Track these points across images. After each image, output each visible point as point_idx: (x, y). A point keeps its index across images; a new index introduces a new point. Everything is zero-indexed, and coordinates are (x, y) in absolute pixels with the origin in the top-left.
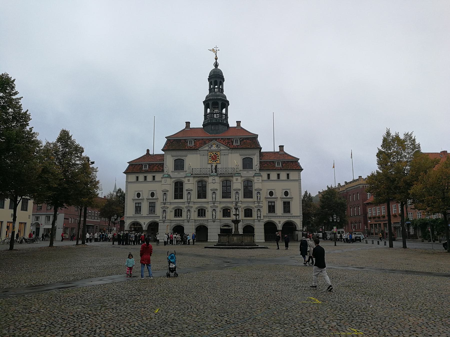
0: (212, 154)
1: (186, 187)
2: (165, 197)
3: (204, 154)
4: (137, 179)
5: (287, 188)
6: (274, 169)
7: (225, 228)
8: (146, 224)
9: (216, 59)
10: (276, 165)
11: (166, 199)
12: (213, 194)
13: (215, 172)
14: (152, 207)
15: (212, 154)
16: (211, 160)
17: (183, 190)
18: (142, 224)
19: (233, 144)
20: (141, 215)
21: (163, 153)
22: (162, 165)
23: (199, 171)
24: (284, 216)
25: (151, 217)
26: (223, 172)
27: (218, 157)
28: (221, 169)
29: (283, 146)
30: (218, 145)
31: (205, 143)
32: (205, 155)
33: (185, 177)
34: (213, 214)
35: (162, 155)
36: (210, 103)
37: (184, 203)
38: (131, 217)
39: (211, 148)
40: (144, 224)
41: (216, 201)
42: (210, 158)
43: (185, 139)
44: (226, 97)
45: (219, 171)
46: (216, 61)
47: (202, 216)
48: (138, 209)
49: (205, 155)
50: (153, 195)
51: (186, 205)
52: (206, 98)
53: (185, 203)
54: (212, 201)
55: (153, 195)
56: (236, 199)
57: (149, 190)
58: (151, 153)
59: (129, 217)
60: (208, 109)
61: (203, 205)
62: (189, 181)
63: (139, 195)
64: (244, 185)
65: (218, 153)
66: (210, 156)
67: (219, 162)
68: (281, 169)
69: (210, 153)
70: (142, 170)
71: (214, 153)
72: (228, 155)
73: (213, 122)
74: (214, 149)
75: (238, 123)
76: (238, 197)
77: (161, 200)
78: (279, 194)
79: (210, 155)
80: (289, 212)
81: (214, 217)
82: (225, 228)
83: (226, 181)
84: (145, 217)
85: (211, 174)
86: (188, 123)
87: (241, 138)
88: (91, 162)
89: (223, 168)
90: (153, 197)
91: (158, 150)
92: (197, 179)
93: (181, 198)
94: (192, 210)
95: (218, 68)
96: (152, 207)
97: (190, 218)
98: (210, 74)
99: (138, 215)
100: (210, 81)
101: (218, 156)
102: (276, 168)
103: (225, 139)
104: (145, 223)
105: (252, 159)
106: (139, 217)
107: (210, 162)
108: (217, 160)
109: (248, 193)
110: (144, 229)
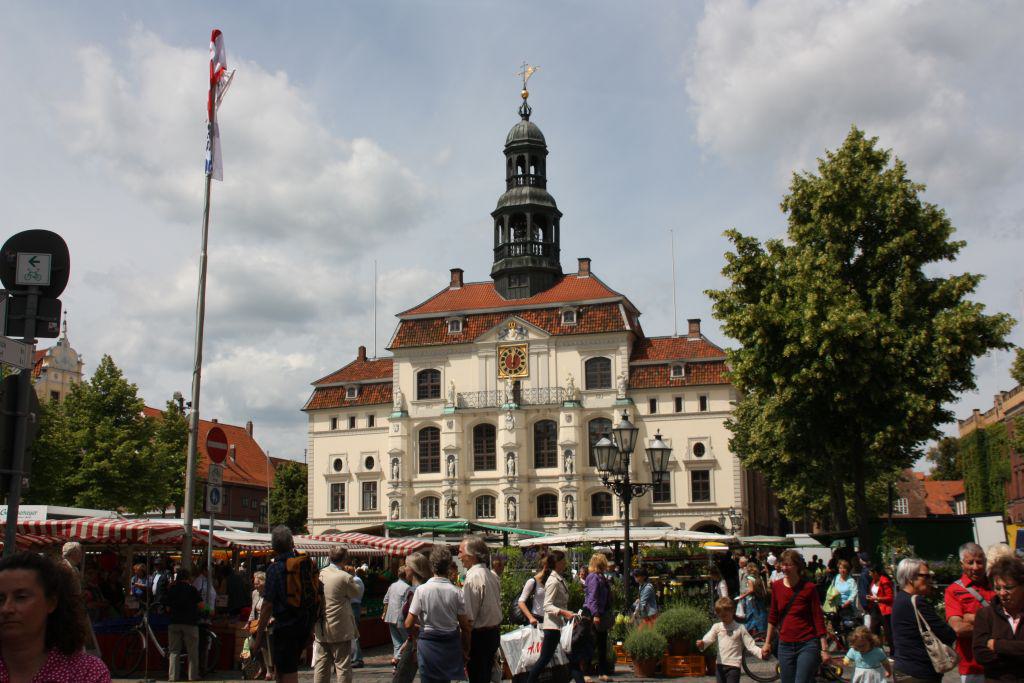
1: (447, 440)
4: (334, 426)
5: (702, 436)
6: (669, 386)
9: (525, 97)
10: (672, 375)
14: (370, 489)
17: (438, 449)
19: (559, 323)
21: (390, 354)
22: (388, 387)
24: (693, 511)
25: (368, 518)
26: (535, 400)
30: (521, 330)
31: (490, 325)
32: (491, 356)
33: (442, 417)
35: (389, 362)
36: (507, 218)
37: (440, 482)
38: (323, 520)
39: (506, 338)
41: (516, 474)
43: (442, 318)
44: (553, 202)
45: (528, 396)
46: (525, 104)
47: (487, 514)
48: (338, 498)
49: (491, 356)
50: (370, 462)
51: (444, 489)
52: (500, 202)
55: (370, 462)
57: (363, 451)
58: (370, 355)
59: (318, 520)
62: (450, 425)
63: (338, 464)
64: (593, 431)
67: (525, 372)
68: (683, 385)
70: (344, 402)
72: (548, 353)
73: (513, 266)
74: (513, 339)
75: (585, 262)
77: (388, 476)
78: (681, 453)
80: (707, 496)
81: (511, 517)
86: (457, 273)
87: (581, 306)
88: (187, 404)
89: (534, 389)
90: (371, 468)
91: (377, 351)
92: (472, 421)
93: (436, 468)
95: (531, 119)
96: (370, 489)
98: (508, 140)
99: (338, 514)
101: (523, 358)
102: (672, 382)
103: (542, 310)
105: (609, 361)
106: (340, 519)
108: (520, 369)
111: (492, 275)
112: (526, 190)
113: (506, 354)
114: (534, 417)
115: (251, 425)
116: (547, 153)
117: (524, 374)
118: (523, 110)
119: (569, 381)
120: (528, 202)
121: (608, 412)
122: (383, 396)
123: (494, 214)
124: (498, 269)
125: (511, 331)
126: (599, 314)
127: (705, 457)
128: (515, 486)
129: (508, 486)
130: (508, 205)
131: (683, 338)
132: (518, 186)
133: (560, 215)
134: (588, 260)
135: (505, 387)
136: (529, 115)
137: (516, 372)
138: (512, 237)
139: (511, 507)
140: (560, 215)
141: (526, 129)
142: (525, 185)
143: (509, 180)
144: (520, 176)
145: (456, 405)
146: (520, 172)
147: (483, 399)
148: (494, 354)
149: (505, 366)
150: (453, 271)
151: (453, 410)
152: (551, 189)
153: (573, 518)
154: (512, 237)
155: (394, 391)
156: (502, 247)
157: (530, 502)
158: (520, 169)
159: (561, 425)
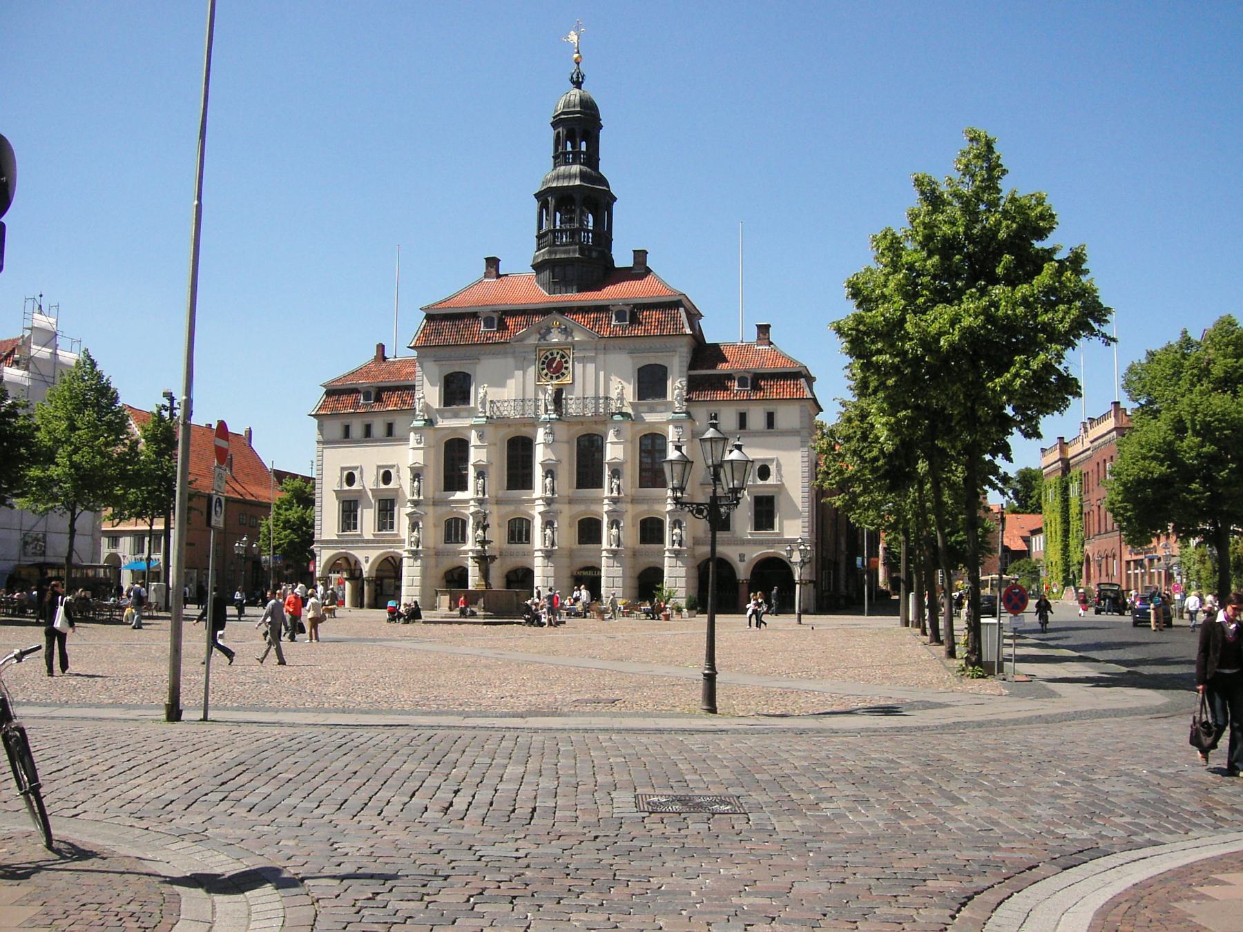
0: (548, 354)
1: (476, 455)
2: (416, 483)
7: (585, 573)
8: (370, 561)
11: (419, 491)
13: (555, 411)
18: (362, 560)
20: (359, 535)
26: (579, 410)
27: (565, 365)
29: (768, 327)
36: (552, 202)
40: (367, 561)
42: (543, 369)
50: (387, 478)
60: (557, 213)
63: (350, 479)
64: (643, 448)
65: (567, 351)
73: (558, 257)
75: (640, 256)
76: (619, 486)
79: (543, 359)
82: (585, 573)
84: (368, 541)
85: (543, 416)
93: (464, 487)
94: (492, 521)
100: (556, 131)
104: (367, 560)
105: (666, 368)
108: (563, 374)
109: (651, 474)
110: (365, 575)
111: (533, 266)
112: (576, 169)
113: (547, 357)
114: (580, 430)
115: (250, 432)
116: (601, 127)
117: (567, 380)
118: (575, 76)
119: (618, 391)
120: (578, 182)
121: (662, 426)
122: (404, 402)
123: (537, 196)
124: (540, 260)
125: (555, 332)
126: (656, 315)
127: (772, 480)
130: (554, 185)
131: (749, 345)
132: (567, 163)
133: (615, 199)
134: (645, 252)
135: (546, 397)
136: (582, 82)
137: (558, 378)
138: (558, 223)
139: (548, 531)
140: (615, 199)
141: (578, 98)
142: (574, 163)
143: (555, 158)
144: (569, 153)
145: (488, 414)
146: (569, 149)
147: (519, 408)
149: (545, 371)
150: (487, 259)
151: (485, 419)
152: (603, 169)
154: (558, 223)
155: (417, 396)
156: (545, 234)
157: (570, 526)
158: (569, 144)
159: (609, 440)
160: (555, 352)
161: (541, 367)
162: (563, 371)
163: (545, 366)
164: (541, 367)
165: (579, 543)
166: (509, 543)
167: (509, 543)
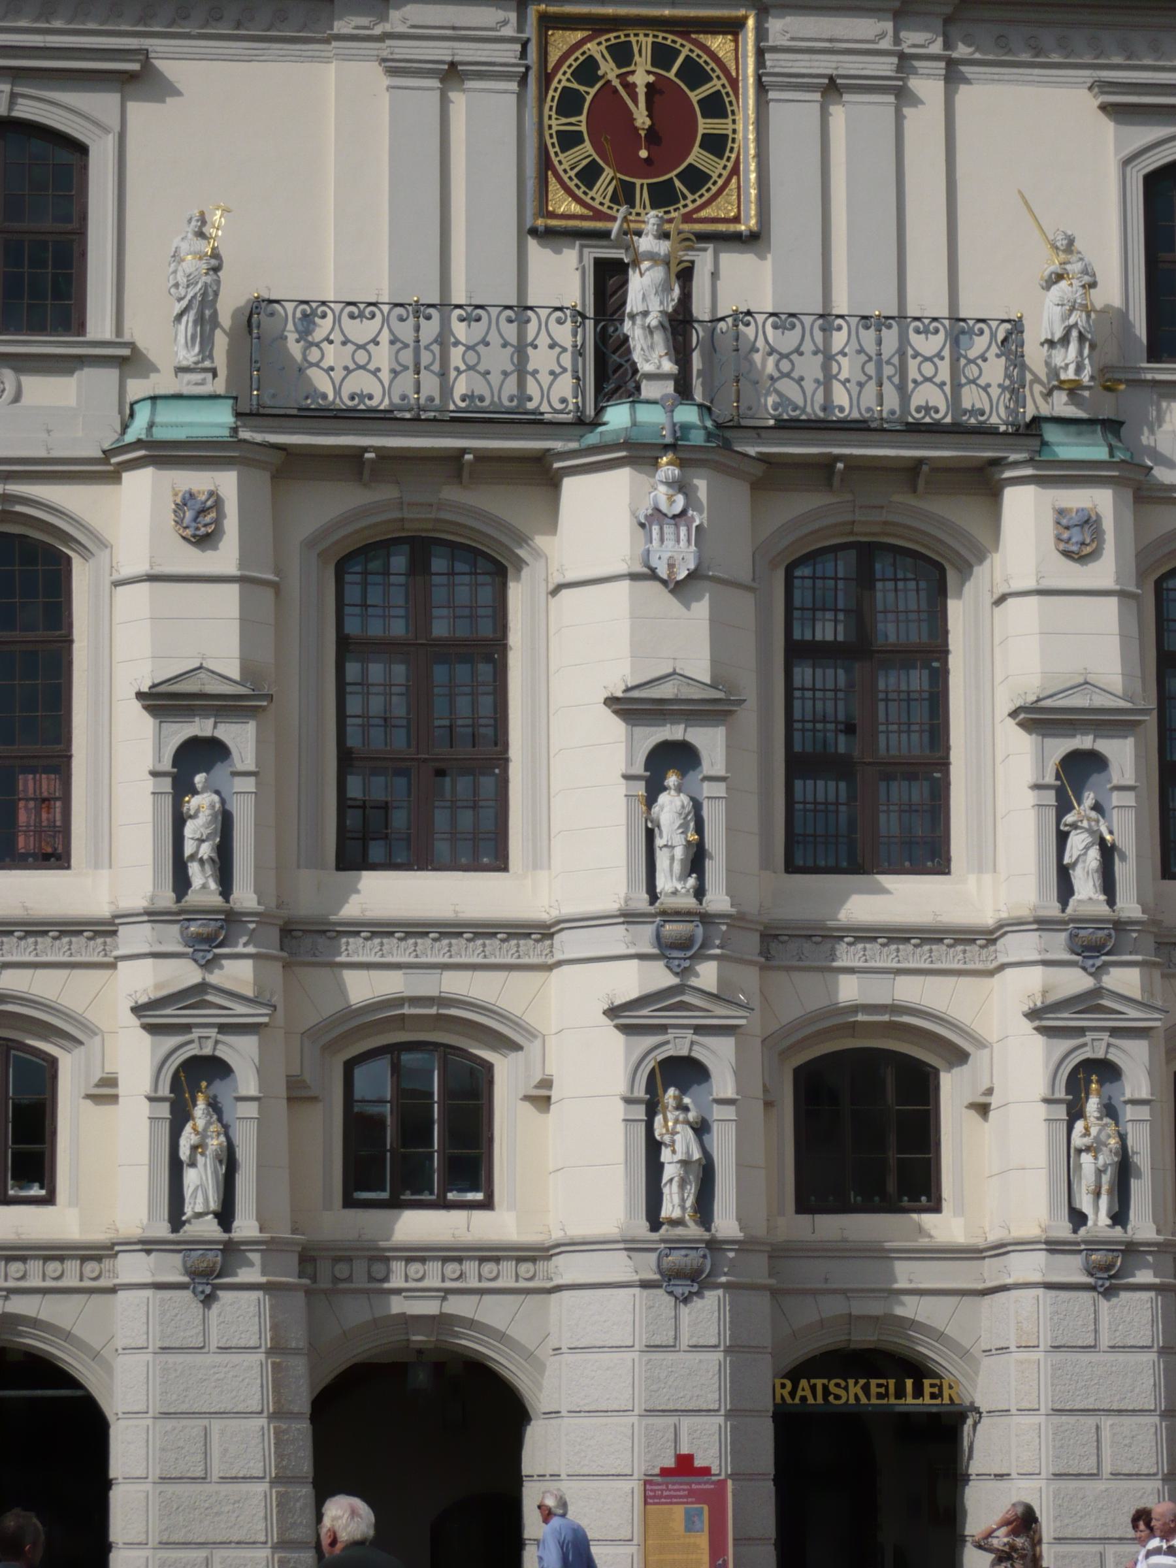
3: (467, 52)
12: (654, 789)
15: (609, 69)
16: (589, 175)
23: (382, 356)
27: (704, 126)
28: (787, 341)
34: (653, 1147)
42: (568, 140)
53: (134, 938)
54: (641, 901)
56: (1064, 875)
61: (454, 984)
66: (569, 103)
69: (561, 41)
71: (643, 43)
79: (562, 80)
83: (844, 566)
97: (225, 1216)
107: (562, 204)
108: (696, 179)
113: (587, 71)
128: (707, 975)
129: (661, 977)
137: (663, 197)
148: (508, 54)
153: (1119, 1217)
160: (643, 43)
161: (557, 124)
162: (697, 156)
163: (581, 122)
164: (557, 124)
165: (803, 1207)
166: (349, 1202)
167: (349, 1202)
